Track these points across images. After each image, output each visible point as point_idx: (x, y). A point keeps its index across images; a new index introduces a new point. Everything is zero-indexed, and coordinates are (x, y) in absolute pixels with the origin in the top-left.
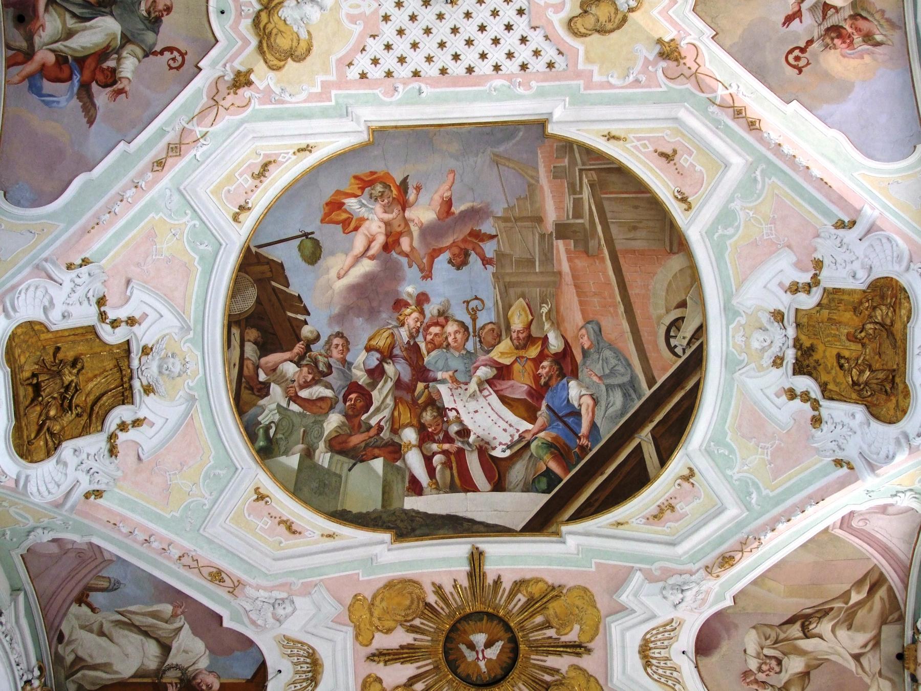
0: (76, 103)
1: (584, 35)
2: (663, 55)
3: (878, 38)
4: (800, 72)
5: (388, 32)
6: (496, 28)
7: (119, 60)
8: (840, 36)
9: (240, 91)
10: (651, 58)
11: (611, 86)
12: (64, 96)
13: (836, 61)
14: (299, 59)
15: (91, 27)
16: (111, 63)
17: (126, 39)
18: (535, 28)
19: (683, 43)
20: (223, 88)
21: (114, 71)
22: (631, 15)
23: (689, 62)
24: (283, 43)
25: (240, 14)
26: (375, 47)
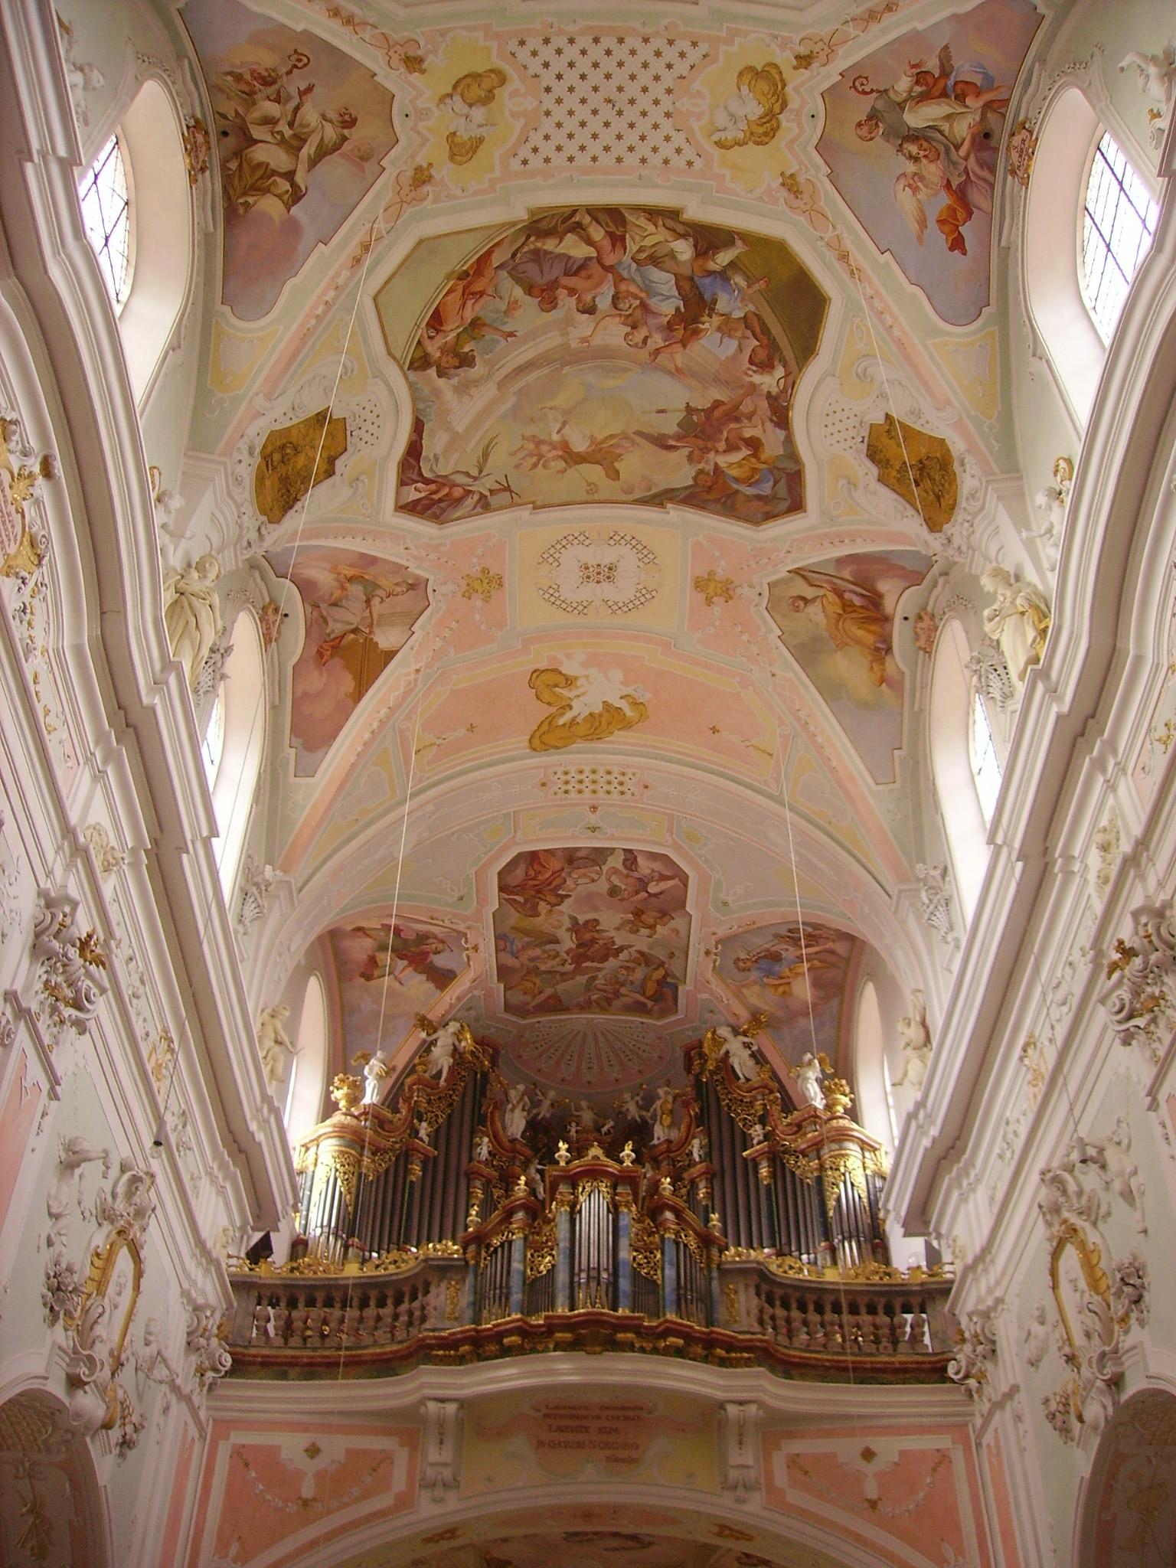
0: (956, 63)
1: (492, 71)
2: (420, 60)
3: (229, 78)
4: (296, 51)
5: (668, 79)
6: (572, 77)
7: (911, 90)
8: (263, 78)
9: (807, 53)
10: (431, 56)
11: (468, 29)
12: (964, 69)
13: (265, 60)
14: (750, 69)
15: (928, 120)
16: (918, 89)
17: (901, 106)
18: (536, 76)
19: (402, 70)
20: (823, 57)
21: (917, 83)
22: (450, 91)
23: (395, 58)
24: (763, 86)
25: (798, 112)
26: (681, 67)
